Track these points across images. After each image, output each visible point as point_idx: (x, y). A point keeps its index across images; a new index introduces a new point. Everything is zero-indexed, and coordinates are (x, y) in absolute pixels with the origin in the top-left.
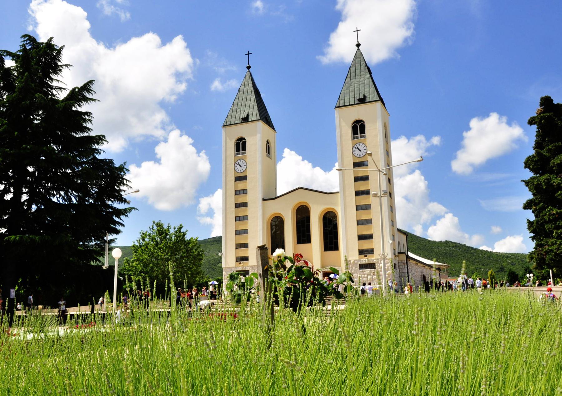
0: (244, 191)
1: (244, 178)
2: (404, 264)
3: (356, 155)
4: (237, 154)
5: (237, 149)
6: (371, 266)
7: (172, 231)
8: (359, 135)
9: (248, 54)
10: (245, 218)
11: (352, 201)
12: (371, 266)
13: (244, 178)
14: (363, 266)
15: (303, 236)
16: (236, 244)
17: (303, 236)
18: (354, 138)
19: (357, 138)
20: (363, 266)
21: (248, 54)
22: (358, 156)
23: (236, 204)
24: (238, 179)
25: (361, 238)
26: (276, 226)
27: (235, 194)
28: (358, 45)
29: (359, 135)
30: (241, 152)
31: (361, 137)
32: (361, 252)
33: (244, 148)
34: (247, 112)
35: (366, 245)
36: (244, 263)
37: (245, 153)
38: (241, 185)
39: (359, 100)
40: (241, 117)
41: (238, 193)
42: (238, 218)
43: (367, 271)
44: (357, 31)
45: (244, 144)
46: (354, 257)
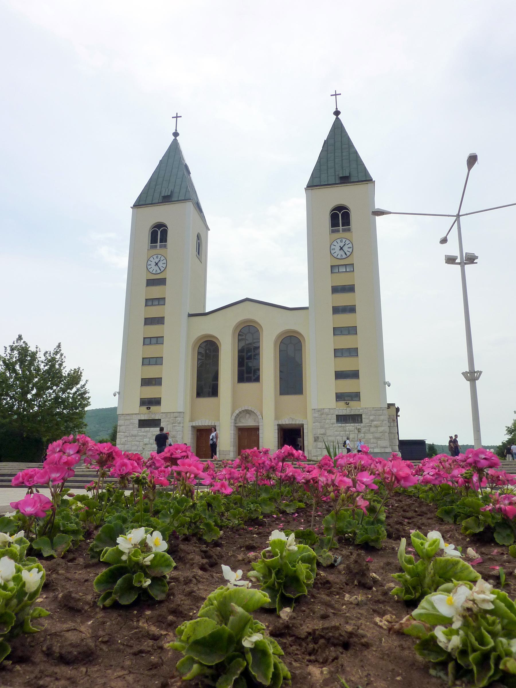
0: (161, 301)
1: (162, 282)
2: (394, 420)
3: (335, 255)
4: (152, 247)
5: (153, 240)
6: (356, 418)
7: (41, 357)
8: (341, 227)
9: (177, 117)
10: (158, 340)
11: (330, 321)
12: (356, 418)
13: (162, 282)
14: (342, 419)
15: (248, 370)
16: (142, 379)
17: (248, 370)
18: (333, 231)
19: (338, 231)
20: (342, 419)
21: (177, 117)
22: (339, 257)
23: (146, 319)
24: (151, 283)
25: (340, 375)
26: (207, 353)
27: (146, 305)
28: (337, 113)
29: (341, 227)
30: (159, 244)
31: (344, 230)
32: (340, 397)
33: (164, 239)
34: (171, 188)
35: (347, 386)
36: (153, 408)
37: (165, 246)
38: (156, 292)
39: (342, 178)
40: (163, 195)
41: (150, 303)
42: (147, 341)
43: (350, 427)
44: (336, 95)
45: (165, 233)
46: (330, 404)
